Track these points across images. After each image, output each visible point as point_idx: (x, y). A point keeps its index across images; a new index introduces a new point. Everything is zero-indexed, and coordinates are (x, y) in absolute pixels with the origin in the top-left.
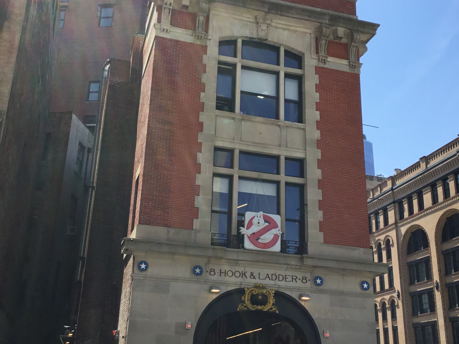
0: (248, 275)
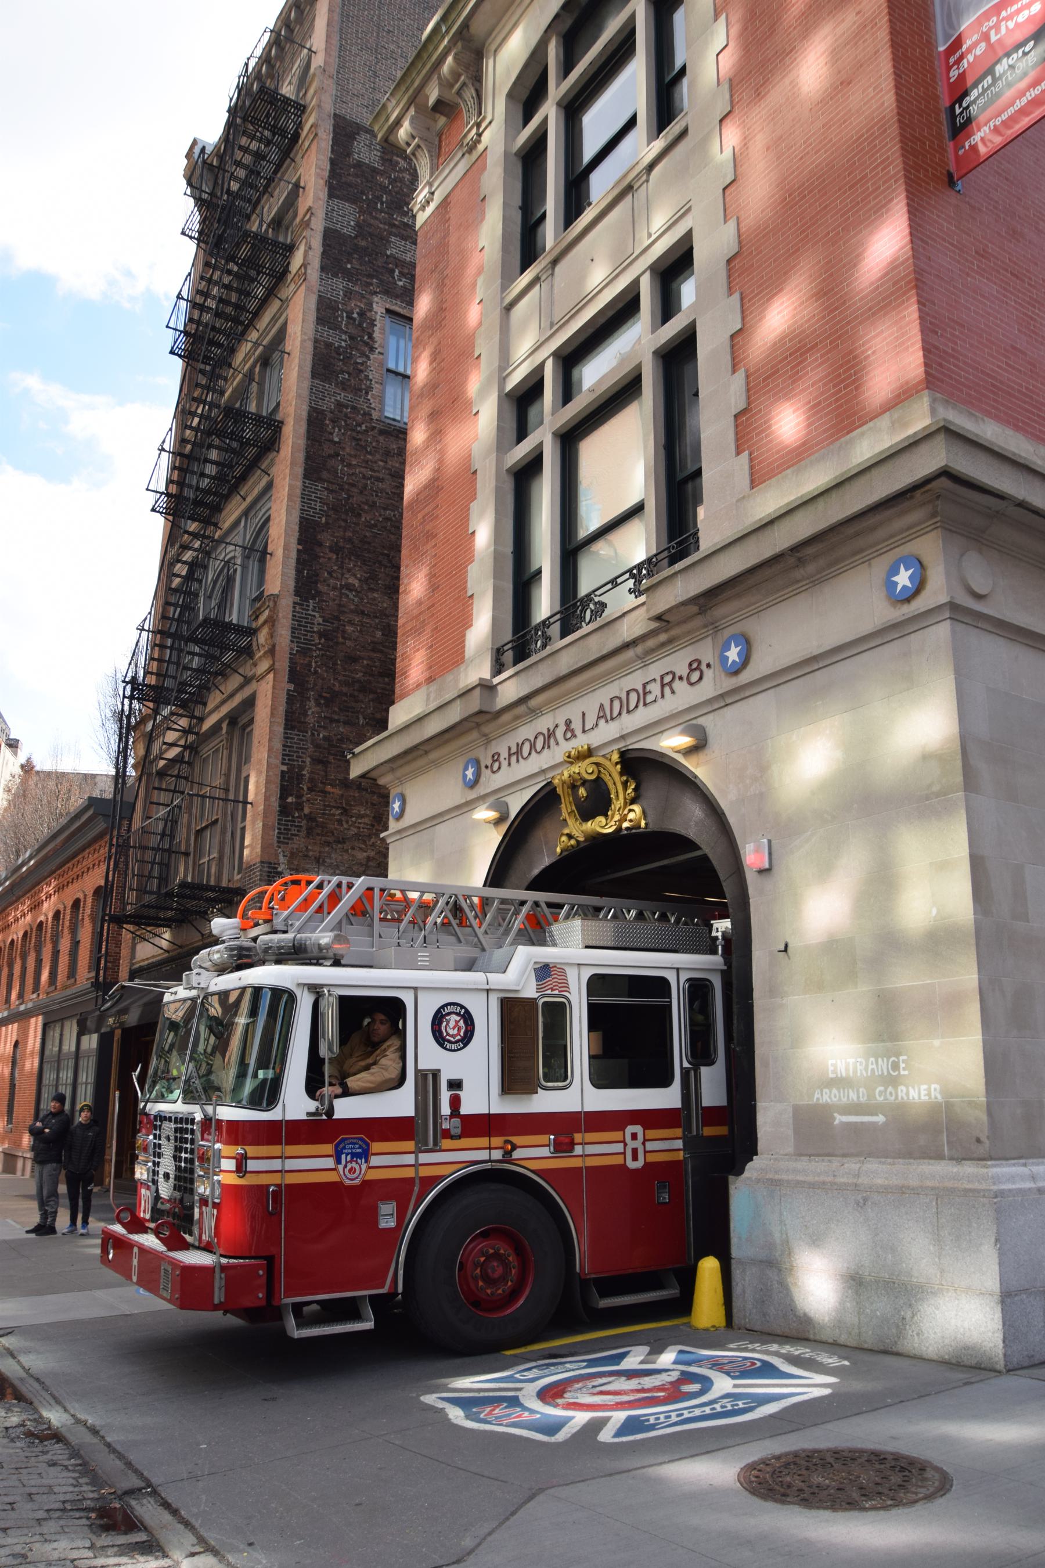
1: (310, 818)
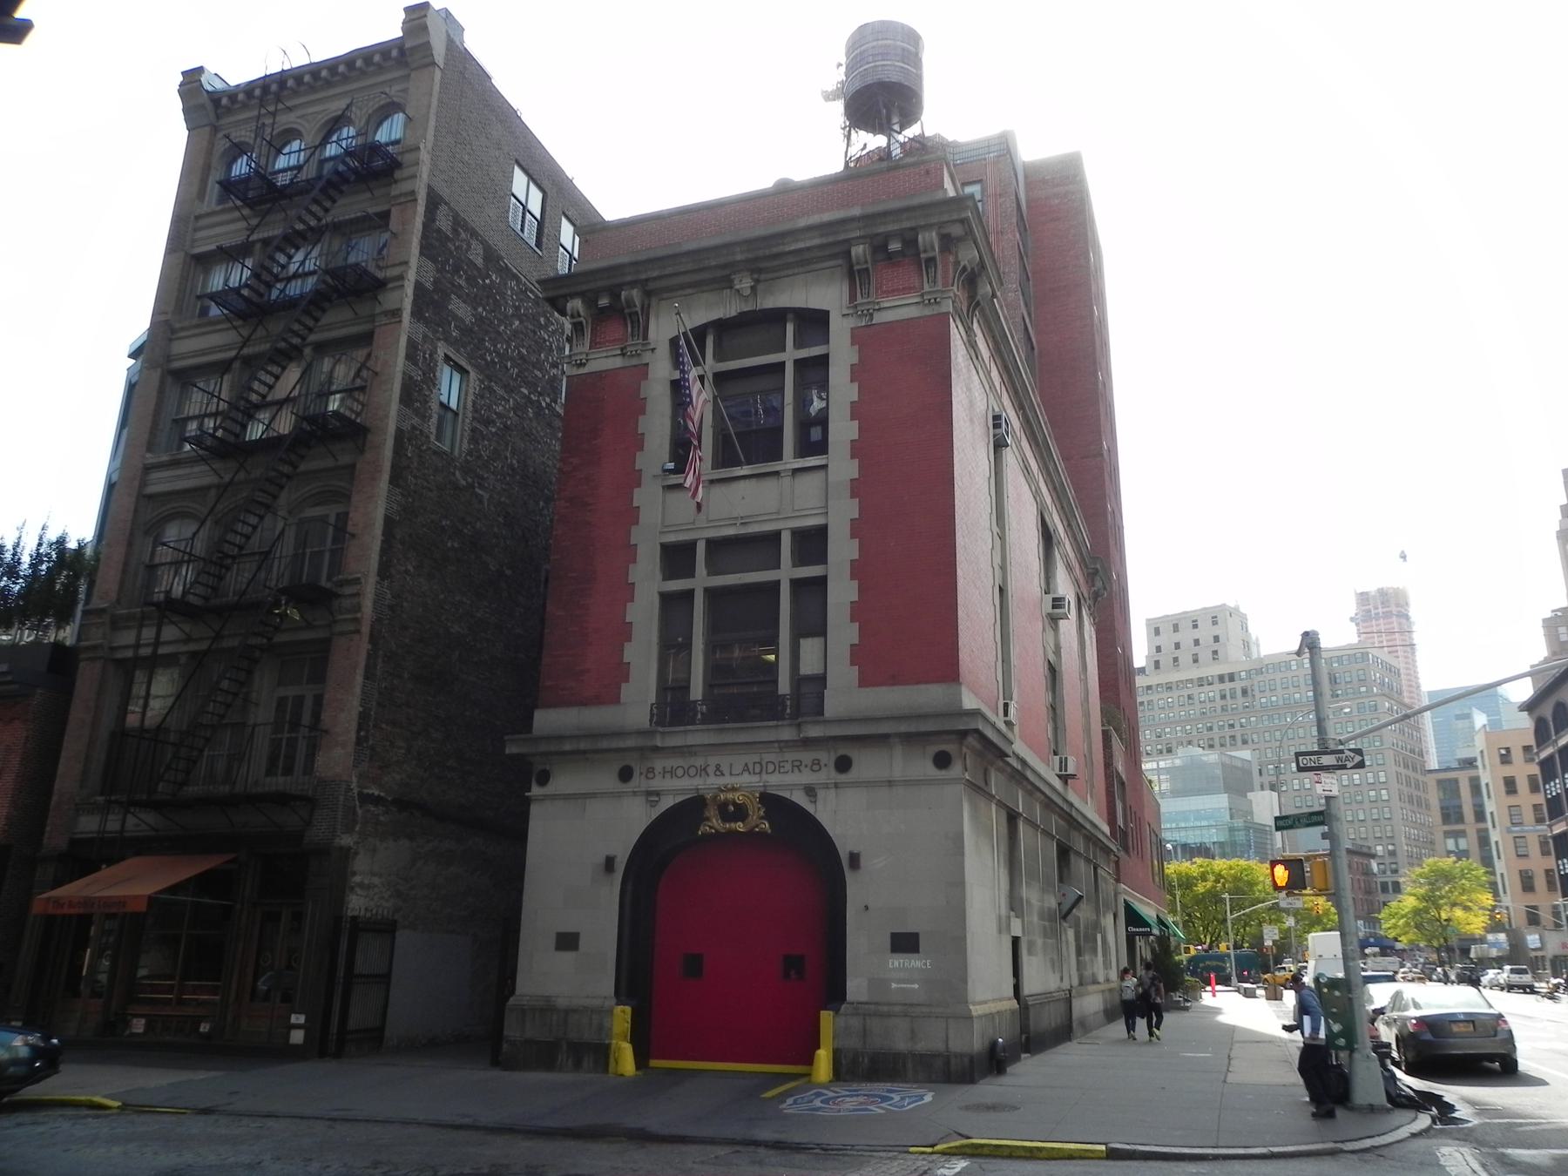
0: (711, 770)
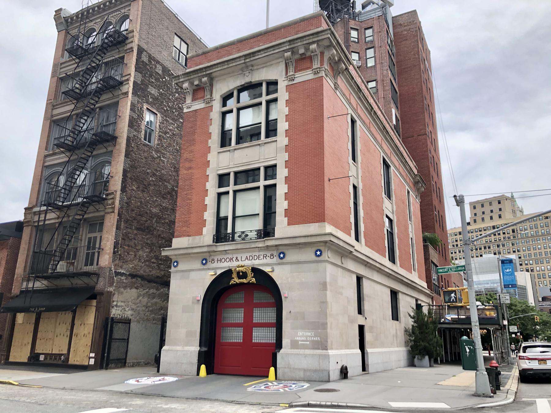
0: (234, 259)
1: (120, 255)
